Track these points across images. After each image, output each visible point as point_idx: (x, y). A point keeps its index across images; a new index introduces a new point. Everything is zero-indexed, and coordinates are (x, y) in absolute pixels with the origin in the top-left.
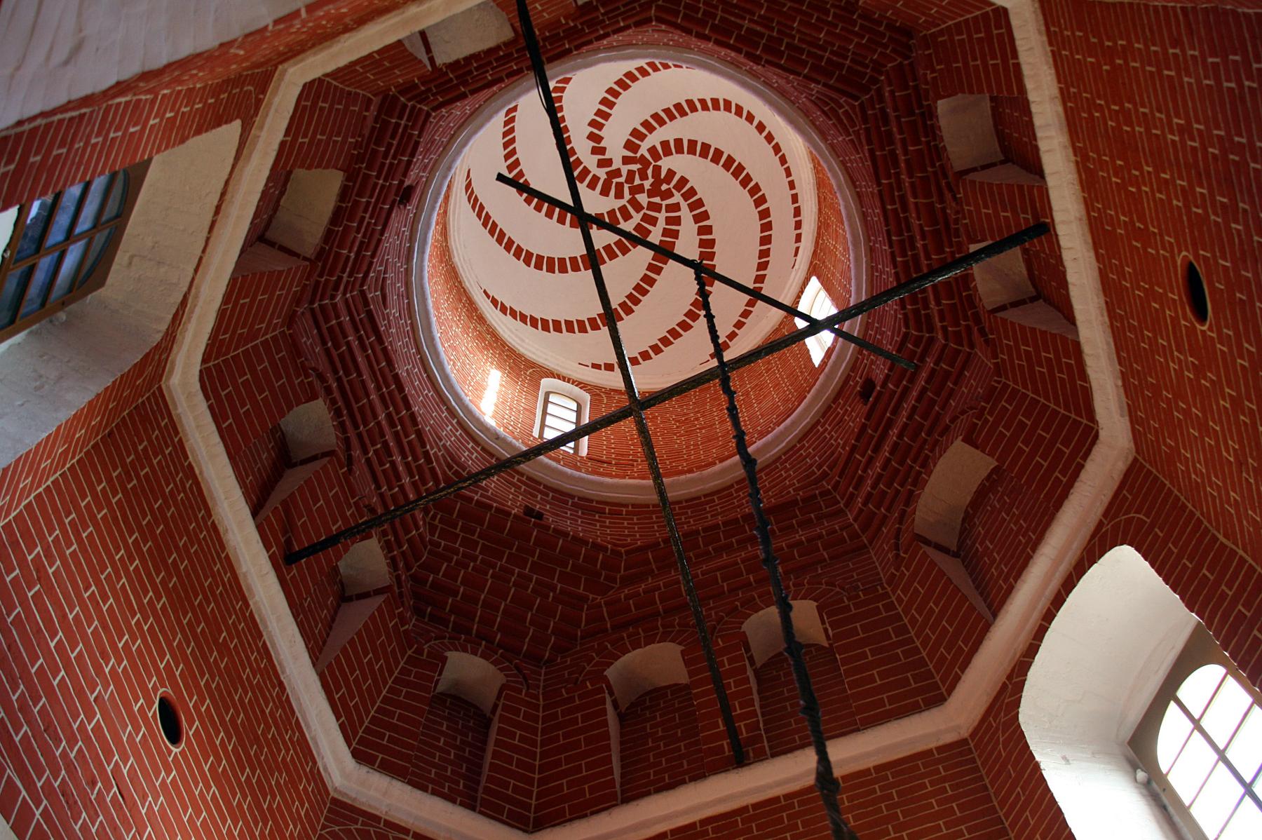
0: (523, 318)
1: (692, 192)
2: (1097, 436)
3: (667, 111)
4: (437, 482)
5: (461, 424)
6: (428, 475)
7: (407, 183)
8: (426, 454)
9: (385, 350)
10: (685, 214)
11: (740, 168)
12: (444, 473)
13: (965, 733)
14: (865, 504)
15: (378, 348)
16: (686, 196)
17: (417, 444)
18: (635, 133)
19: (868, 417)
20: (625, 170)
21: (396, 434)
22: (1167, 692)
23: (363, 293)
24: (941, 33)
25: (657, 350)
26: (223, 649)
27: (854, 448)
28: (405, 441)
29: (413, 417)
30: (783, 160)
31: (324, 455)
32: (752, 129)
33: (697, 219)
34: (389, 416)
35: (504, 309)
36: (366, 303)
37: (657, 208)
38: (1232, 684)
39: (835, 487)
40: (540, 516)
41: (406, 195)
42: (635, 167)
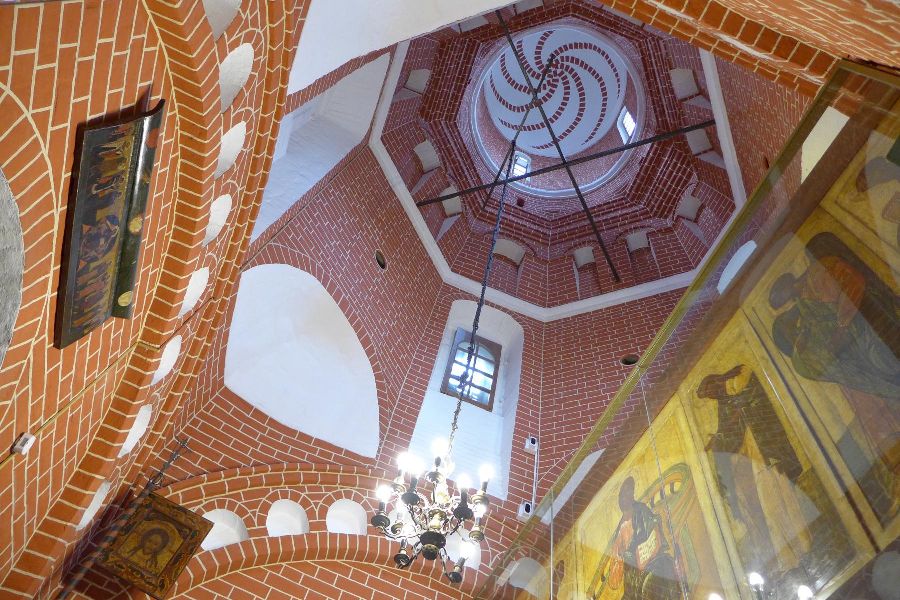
4: (624, 198)
5: (608, 183)
6: (620, 202)
7: (515, 205)
9: (573, 215)
10: (565, 54)
12: (622, 195)
16: (558, 54)
17: (609, 206)
21: (603, 214)
25: (615, 70)
28: (606, 211)
29: (599, 206)
33: (567, 49)
36: (556, 220)
37: (563, 66)
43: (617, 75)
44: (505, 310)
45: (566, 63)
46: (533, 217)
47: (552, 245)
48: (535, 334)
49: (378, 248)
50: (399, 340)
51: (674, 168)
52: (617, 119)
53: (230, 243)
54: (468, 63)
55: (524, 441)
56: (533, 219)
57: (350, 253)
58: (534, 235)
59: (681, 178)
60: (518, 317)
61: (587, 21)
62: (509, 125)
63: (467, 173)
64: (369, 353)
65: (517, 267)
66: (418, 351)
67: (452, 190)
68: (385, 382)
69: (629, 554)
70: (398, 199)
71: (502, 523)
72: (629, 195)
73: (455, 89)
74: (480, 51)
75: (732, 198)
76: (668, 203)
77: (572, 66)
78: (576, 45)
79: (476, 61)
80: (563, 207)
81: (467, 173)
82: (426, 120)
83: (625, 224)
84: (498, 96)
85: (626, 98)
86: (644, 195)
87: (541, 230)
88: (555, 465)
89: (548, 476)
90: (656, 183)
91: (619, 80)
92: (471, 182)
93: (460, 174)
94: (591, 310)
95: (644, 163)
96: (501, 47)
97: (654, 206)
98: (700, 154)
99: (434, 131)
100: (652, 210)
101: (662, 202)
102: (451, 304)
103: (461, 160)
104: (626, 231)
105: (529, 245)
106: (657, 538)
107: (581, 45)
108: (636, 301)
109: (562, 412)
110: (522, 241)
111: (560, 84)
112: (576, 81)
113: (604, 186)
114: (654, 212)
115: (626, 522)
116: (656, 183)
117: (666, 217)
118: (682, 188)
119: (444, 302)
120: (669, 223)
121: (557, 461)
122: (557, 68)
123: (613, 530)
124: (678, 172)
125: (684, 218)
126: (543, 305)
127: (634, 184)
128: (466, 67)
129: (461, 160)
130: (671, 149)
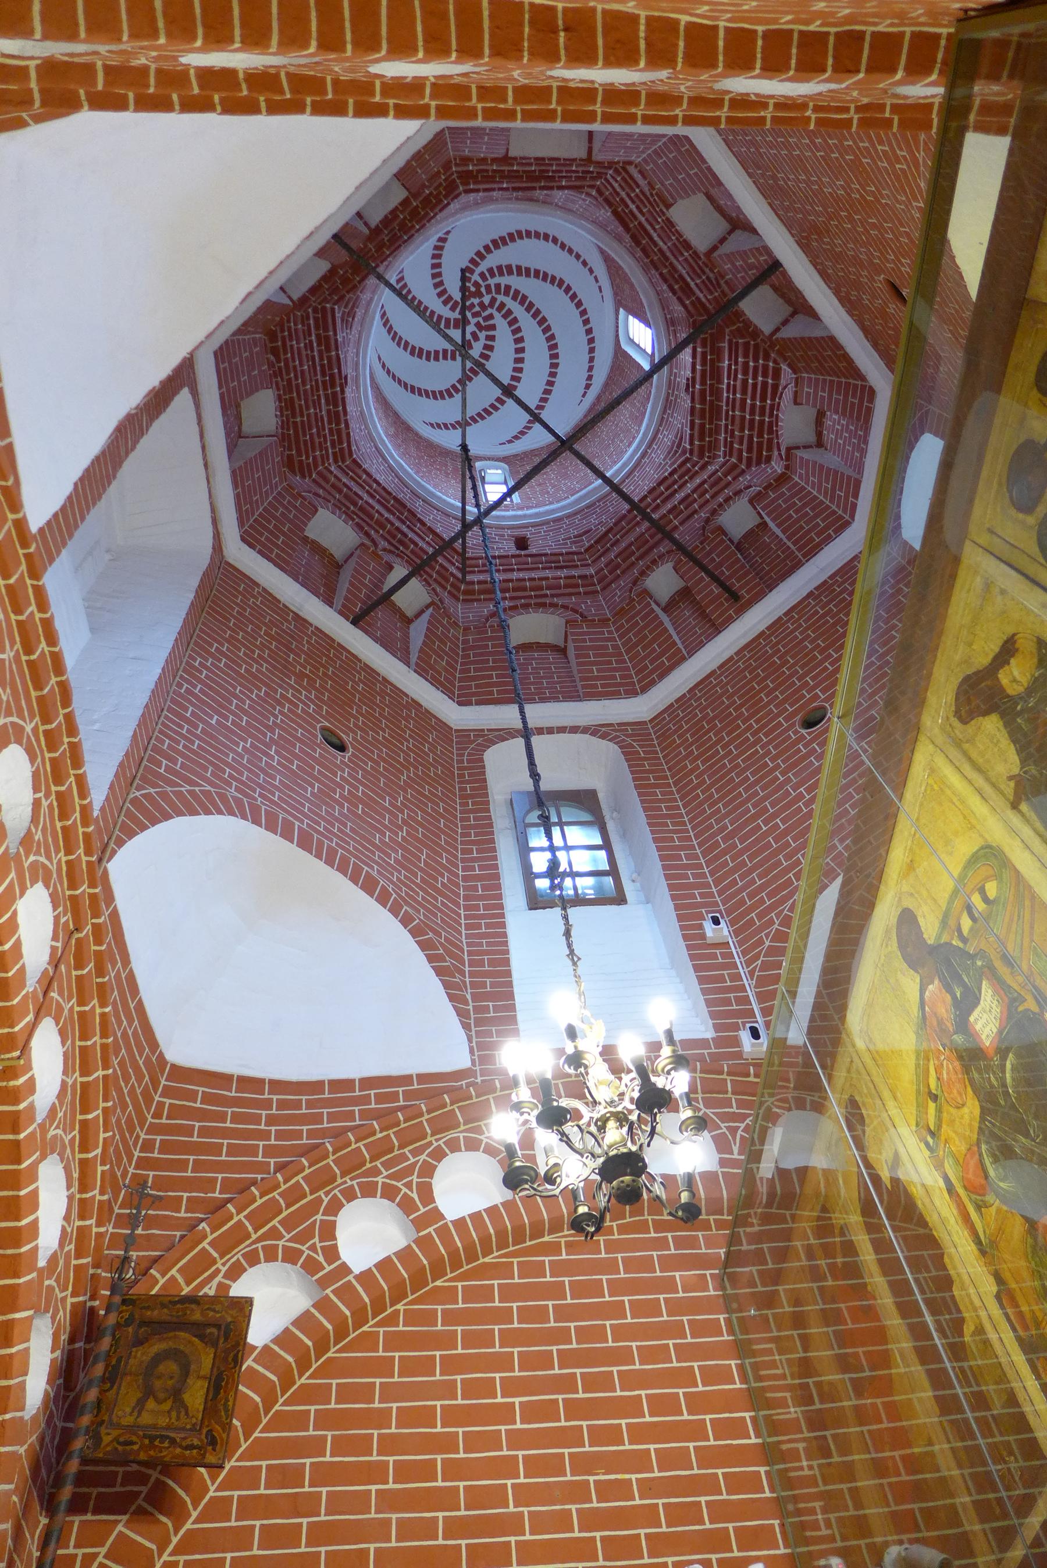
4: (687, 460)
5: (649, 446)
6: (683, 469)
7: (514, 551)
8: (671, 474)
9: (616, 524)
10: (483, 266)
15: (616, 529)
17: (666, 484)
20: (473, 321)
21: (664, 501)
23: (586, 550)
25: (578, 257)
28: (667, 494)
29: (651, 491)
33: (482, 257)
36: (591, 547)
39: (592, 187)
41: (522, 543)
42: (469, 314)
43: (585, 264)
44: (574, 730)
45: (492, 282)
46: (554, 558)
47: (604, 589)
48: (641, 746)
49: (319, 722)
50: (423, 857)
51: (745, 372)
52: (617, 336)
53: (59, 825)
54: (328, 349)
55: (701, 927)
56: (553, 560)
57: (276, 752)
58: (566, 586)
59: (765, 384)
60: (598, 731)
61: (493, 190)
62: (446, 426)
63: (411, 535)
64: (382, 899)
65: (563, 651)
66: (463, 860)
67: (399, 572)
68: (431, 935)
69: (959, 1039)
70: (317, 628)
71: (724, 1076)
72: (691, 452)
73: (328, 403)
74: (338, 321)
75: (863, 378)
76: (760, 435)
77: (504, 280)
78: (494, 242)
79: (340, 339)
80: (593, 520)
81: (411, 535)
82: (303, 476)
83: (708, 501)
84: (406, 386)
85: (616, 294)
87: (574, 572)
88: (767, 943)
89: (765, 966)
90: (727, 412)
91: (591, 271)
92: (425, 546)
93: (400, 542)
94: (714, 665)
95: (694, 386)
96: (372, 299)
97: (740, 451)
98: (777, 330)
99: (324, 489)
100: (740, 459)
101: (751, 437)
102: (482, 761)
103: (391, 517)
104: (714, 512)
105: (565, 607)
106: (996, 992)
107: (503, 239)
108: (780, 619)
109: (741, 853)
110: (552, 605)
111: (499, 320)
112: (522, 303)
113: (644, 455)
114: (744, 461)
115: (931, 987)
116: (727, 412)
117: (769, 459)
118: (773, 399)
119: (469, 761)
120: (777, 467)
121: (767, 935)
123: (915, 1010)
124: (755, 378)
125: (798, 448)
126: (632, 693)
127: (692, 428)
128: (329, 358)
129: (391, 517)
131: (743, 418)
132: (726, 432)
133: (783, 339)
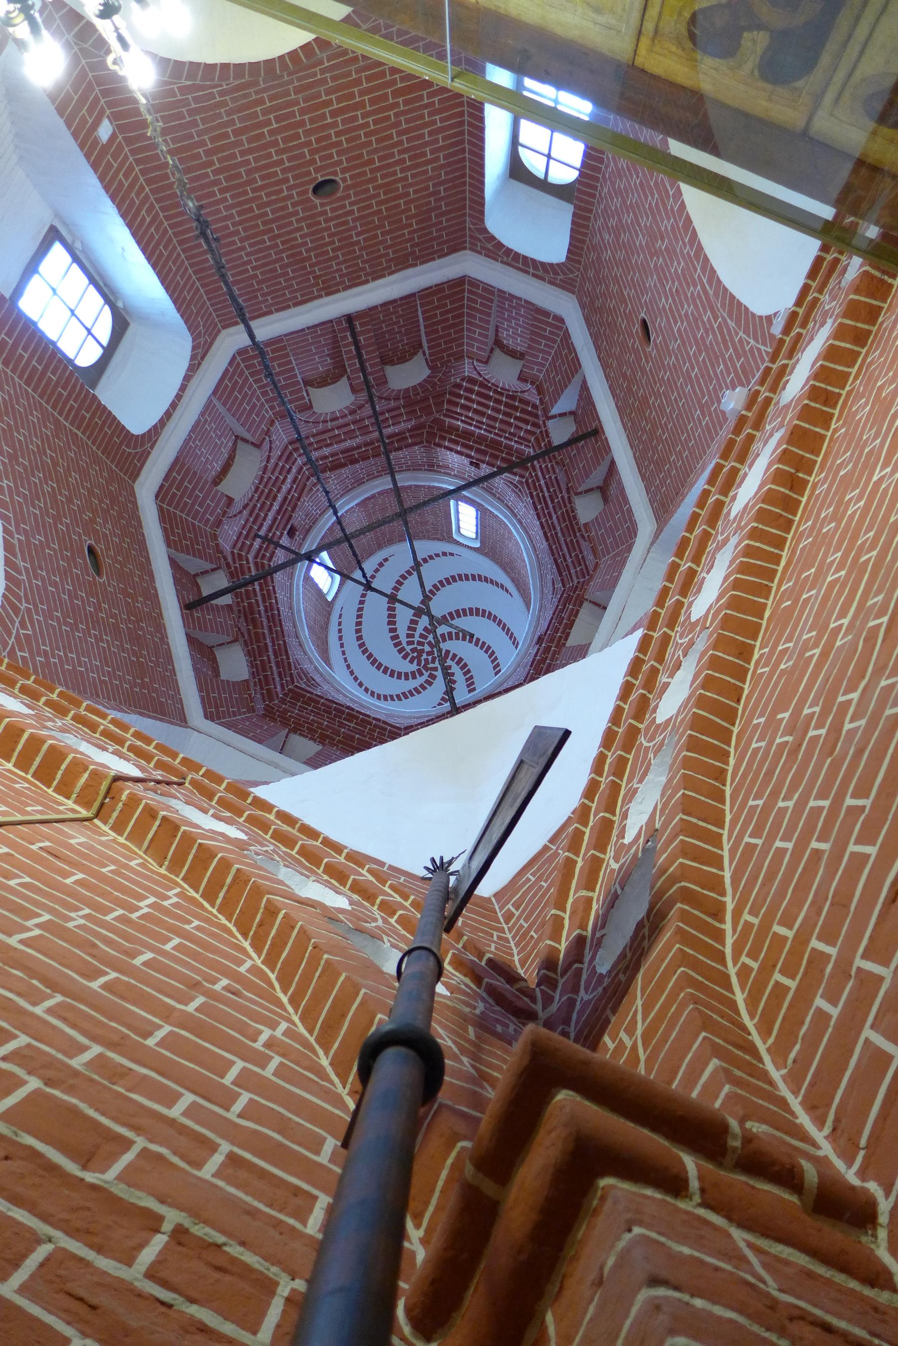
0: (492, 582)
1: (400, 651)
2: (157, 496)
3: (412, 695)
5: (515, 515)
6: (531, 486)
8: (532, 497)
9: (553, 554)
10: (404, 639)
11: (373, 663)
13: (224, 332)
14: (291, 468)
16: (403, 649)
18: (430, 684)
19: (291, 516)
21: (547, 508)
22: (109, 351)
23: (564, 586)
24: (244, 713)
26: (624, 376)
27: (299, 499)
29: (539, 518)
30: (348, 666)
31: (581, 493)
32: (365, 684)
33: (397, 637)
34: (551, 518)
35: (502, 587)
36: (562, 580)
37: (419, 643)
38: (70, 353)
40: (472, 463)
41: (540, 640)
42: (431, 665)
45: (417, 638)
51: (468, 408)
53: (97, 735)
54: (317, 702)
72: (522, 476)
76: (516, 408)
86: (517, 451)
90: (496, 434)
97: (527, 431)
100: (533, 433)
101: (516, 418)
107: (389, 616)
116: (496, 434)
118: (489, 389)
122: (423, 651)
128: (323, 704)
130: (447, 420)
131: (502, 421)
132: (511, 440)
133: (430, 355)
